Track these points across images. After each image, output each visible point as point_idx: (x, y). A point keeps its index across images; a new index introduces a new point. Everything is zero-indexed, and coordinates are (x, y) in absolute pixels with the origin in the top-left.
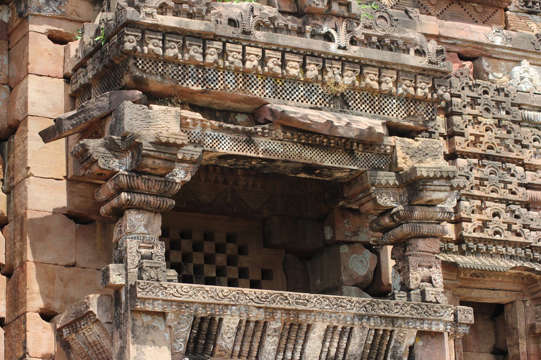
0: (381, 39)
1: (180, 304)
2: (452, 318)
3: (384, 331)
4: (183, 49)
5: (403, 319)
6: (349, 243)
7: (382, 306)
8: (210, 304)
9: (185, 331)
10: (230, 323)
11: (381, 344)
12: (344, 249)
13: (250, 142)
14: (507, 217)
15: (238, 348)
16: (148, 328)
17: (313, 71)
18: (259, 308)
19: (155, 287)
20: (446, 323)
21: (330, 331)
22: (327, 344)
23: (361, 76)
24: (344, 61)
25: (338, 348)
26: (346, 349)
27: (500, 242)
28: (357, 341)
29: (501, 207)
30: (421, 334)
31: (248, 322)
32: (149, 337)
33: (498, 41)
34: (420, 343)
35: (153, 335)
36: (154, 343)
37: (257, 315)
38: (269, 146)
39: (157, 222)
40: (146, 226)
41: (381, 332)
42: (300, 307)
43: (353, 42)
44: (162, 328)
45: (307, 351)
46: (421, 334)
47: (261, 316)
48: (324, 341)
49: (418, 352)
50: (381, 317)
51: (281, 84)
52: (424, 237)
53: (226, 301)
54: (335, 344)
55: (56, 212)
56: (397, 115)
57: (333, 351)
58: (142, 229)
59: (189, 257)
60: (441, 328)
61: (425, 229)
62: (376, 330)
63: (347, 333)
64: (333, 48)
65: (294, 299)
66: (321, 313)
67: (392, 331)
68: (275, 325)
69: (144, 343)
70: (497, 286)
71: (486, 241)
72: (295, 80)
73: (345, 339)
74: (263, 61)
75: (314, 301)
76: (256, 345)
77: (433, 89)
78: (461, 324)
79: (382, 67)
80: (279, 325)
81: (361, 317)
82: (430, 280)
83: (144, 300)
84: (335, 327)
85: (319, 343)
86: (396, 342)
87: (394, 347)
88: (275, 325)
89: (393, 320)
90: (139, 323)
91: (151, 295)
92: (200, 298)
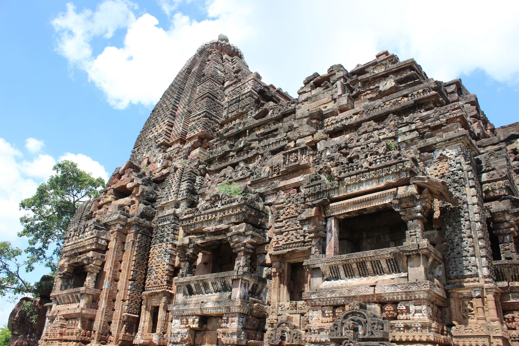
0: (228, 201)
4: (189, 222)
6: (259, 254)
13: (204, 239)
14: (295, 234)
17: (214, 216)
23: (224, 213)
24: (220, 211)
27: (293, 243)
29: (293, 232)
33: (301, 180)
38: (208, 238)
43: (223, 205)
51: (208, 222)
52: (240, 251)
56: (233, 220)
61: (238, 249)
64: (217, 209)
68: (201, 284)
70: (299, 256)
71: (287, 244)
72: (211, 220)
74: (204, 218)
77: (241, 210)
79: (228, 209)
81: (216, 278)
89: (223, 278)
92: (185, 281)
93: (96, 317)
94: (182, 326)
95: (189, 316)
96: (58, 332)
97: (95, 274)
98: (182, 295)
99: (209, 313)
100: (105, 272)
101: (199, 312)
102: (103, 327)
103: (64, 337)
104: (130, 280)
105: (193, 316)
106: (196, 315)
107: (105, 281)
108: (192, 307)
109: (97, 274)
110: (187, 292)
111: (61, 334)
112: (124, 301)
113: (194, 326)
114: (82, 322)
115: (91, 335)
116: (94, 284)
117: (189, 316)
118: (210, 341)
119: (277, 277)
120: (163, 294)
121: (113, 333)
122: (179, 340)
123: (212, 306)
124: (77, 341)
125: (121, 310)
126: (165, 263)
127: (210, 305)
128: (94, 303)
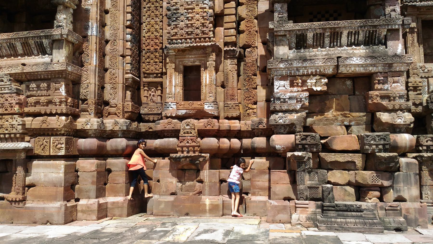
1: (290, 31)
2: (401, 23)
3: (373, 31)
5: (380, 25)
7: (370, 22)
8: (301, 29)
9: (294, 40)
10: (310, 35)
11: (372, 36)
12: (372, 7)
15: (315, 44)
16: (281, 41)
18: (319, 28)
19: (281, 27)
20: (399, 25)
21: (350, 34)
22: (350, 38)
25: (355, 39)
26: (358, 39)
28: (362, 36)
30: (388, 30)
31: (317, 34)
32: (281, 43)
34: (389, 34)
35: (284, 43)
36: (283, 45)
37: (319, 31)
39: (286, 6)
40: (281, 8)
41: (371, 32)
42: (335, 26)
44: (286, 40)
45: (342, 42)
46: (388, 30)
47: (321, 31)
48: (348, 38)
49: (388, 37)
50: (370, 26)
53: (307, 28)
54: (353, 38)
55: (266, 11)
57: (353, 40)
58: (279, 9)
59: (294, 15)
60: (397, 27)
62: (369, 31)
63: (357, 33)
65: (332, 24)
66: (345, 27)
67: (376, 31)
68: (327, 34)
69: (279, 45)
73: (357, 36)
75: (342, 23)
76: (322, 42)
78: (406, 25)
80: (329, 33)
81: (361, 27)
82: (394, 10)
83: (276, 31)
84: (352, 32)
85: (346, 38)
86: (378, 34)
87: (378, 36)
88: (327, 34)
89: (375, 26)
90: (277, 39)
91: (279, 29)
93: (83, 79)
94: (295, 89)
95: (308, 75)
96: (14, 102)
97: (72, 11)
98: (287, 48)
99: (350, 71)
100: (87, 11)
101: (330, 71)
102: (98, 94)
103: (26, 110)
104: (127, 27)
105: (315, 75)
106: (323, 75)
107: (90, 24)
108: (319, 63)
109: (74, 10)
110: (293, 45)
111: (20, 104)
112: (123, 56)
113: (319, 89)
114: (67, 86)
115: (78, 105)
116: (71, 27)
117: (308, 75)
118: (338, 107)
119: (415, 33)
120: (210, 50)
121: (112, 102)
122: (298, 107)
123: (361, 63)
124: (66, 115)
125: (120, 71)
126: (205, 6)
127: (356, 61)
128: (77, 56)
